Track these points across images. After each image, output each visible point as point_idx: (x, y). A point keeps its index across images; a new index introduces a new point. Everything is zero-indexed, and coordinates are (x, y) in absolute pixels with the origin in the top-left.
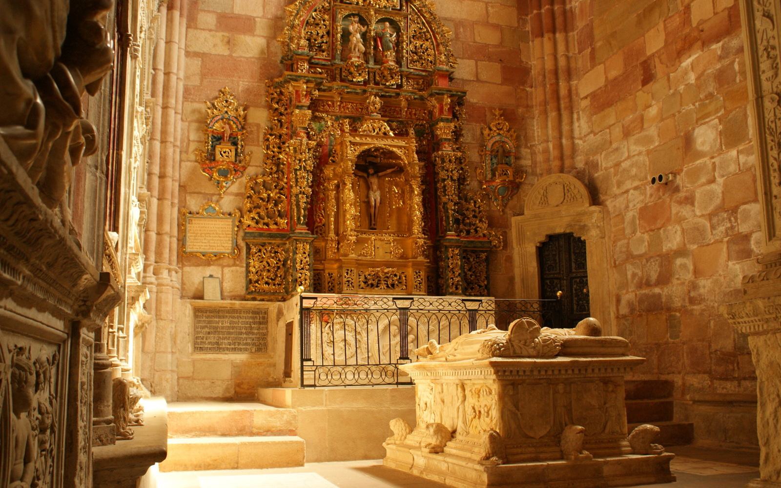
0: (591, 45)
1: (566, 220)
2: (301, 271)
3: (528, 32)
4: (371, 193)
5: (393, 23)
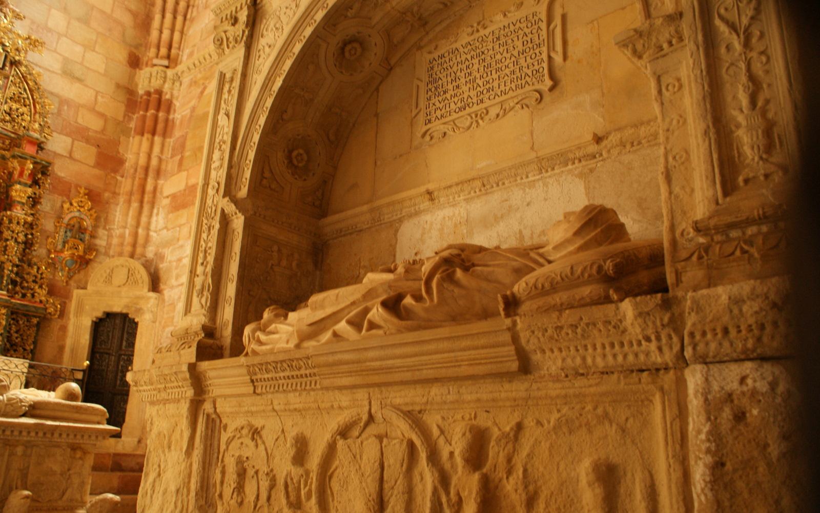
0: (182, 153)
1: (125, 301)
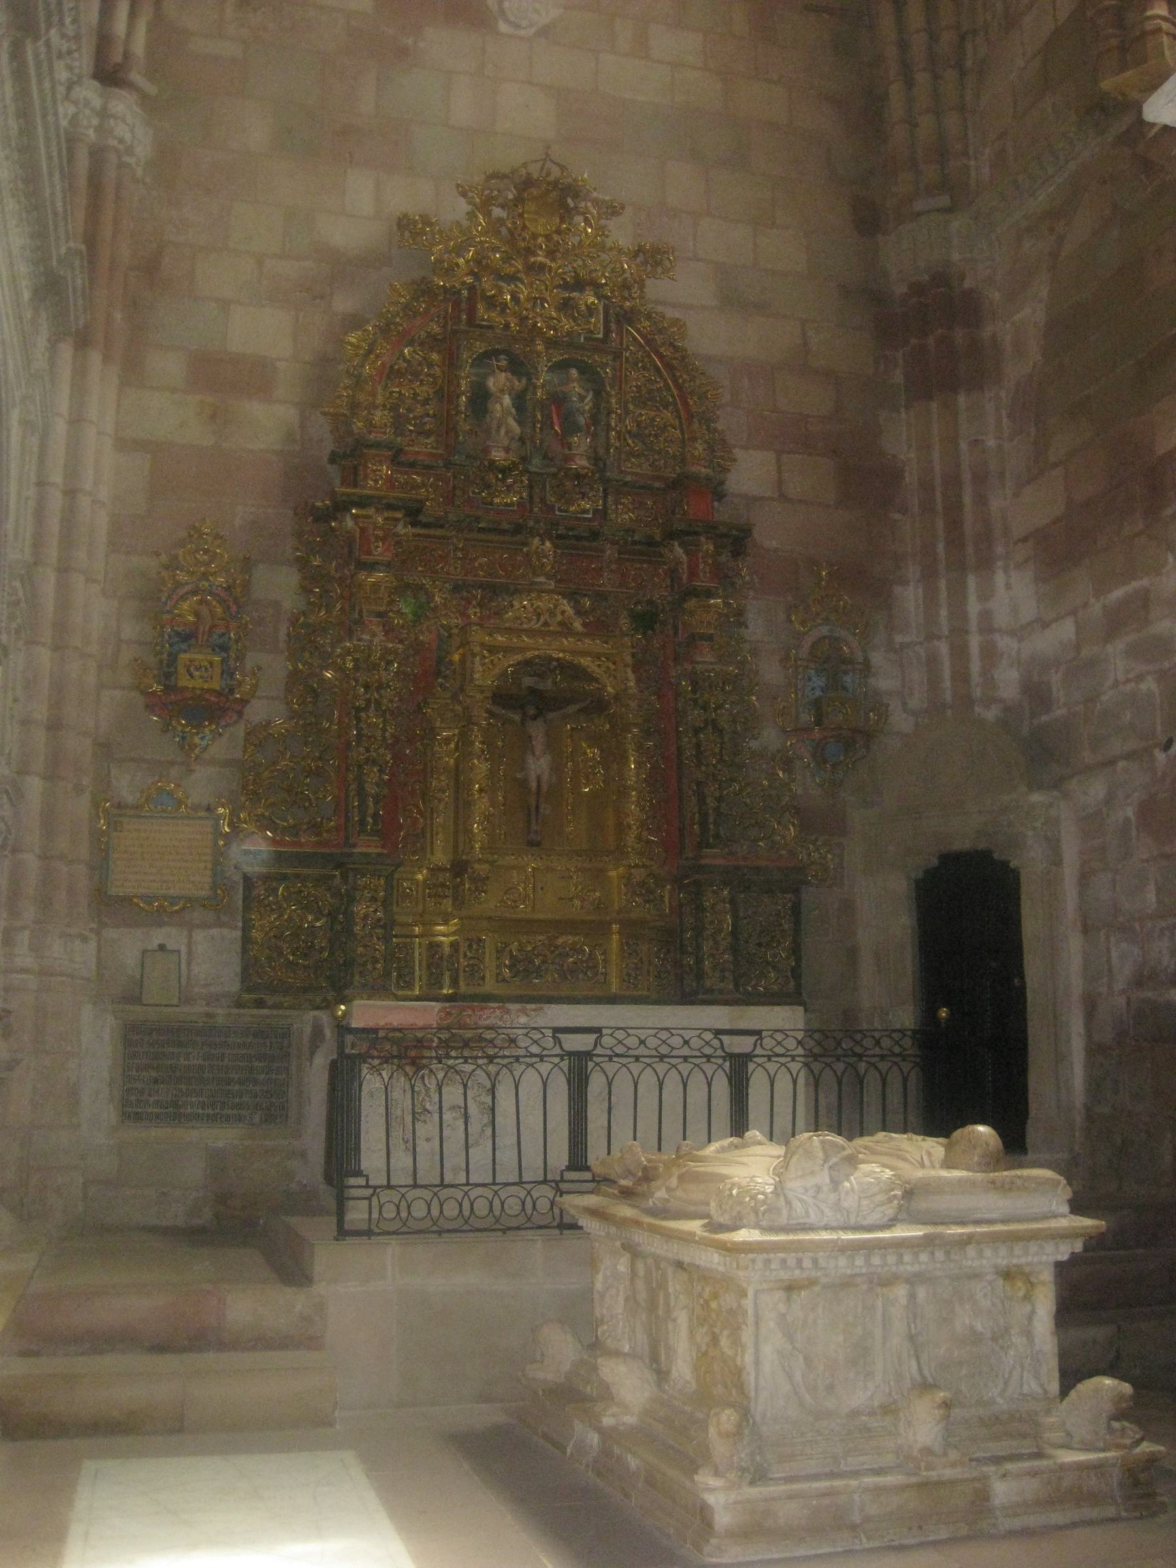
5: (584, 369)
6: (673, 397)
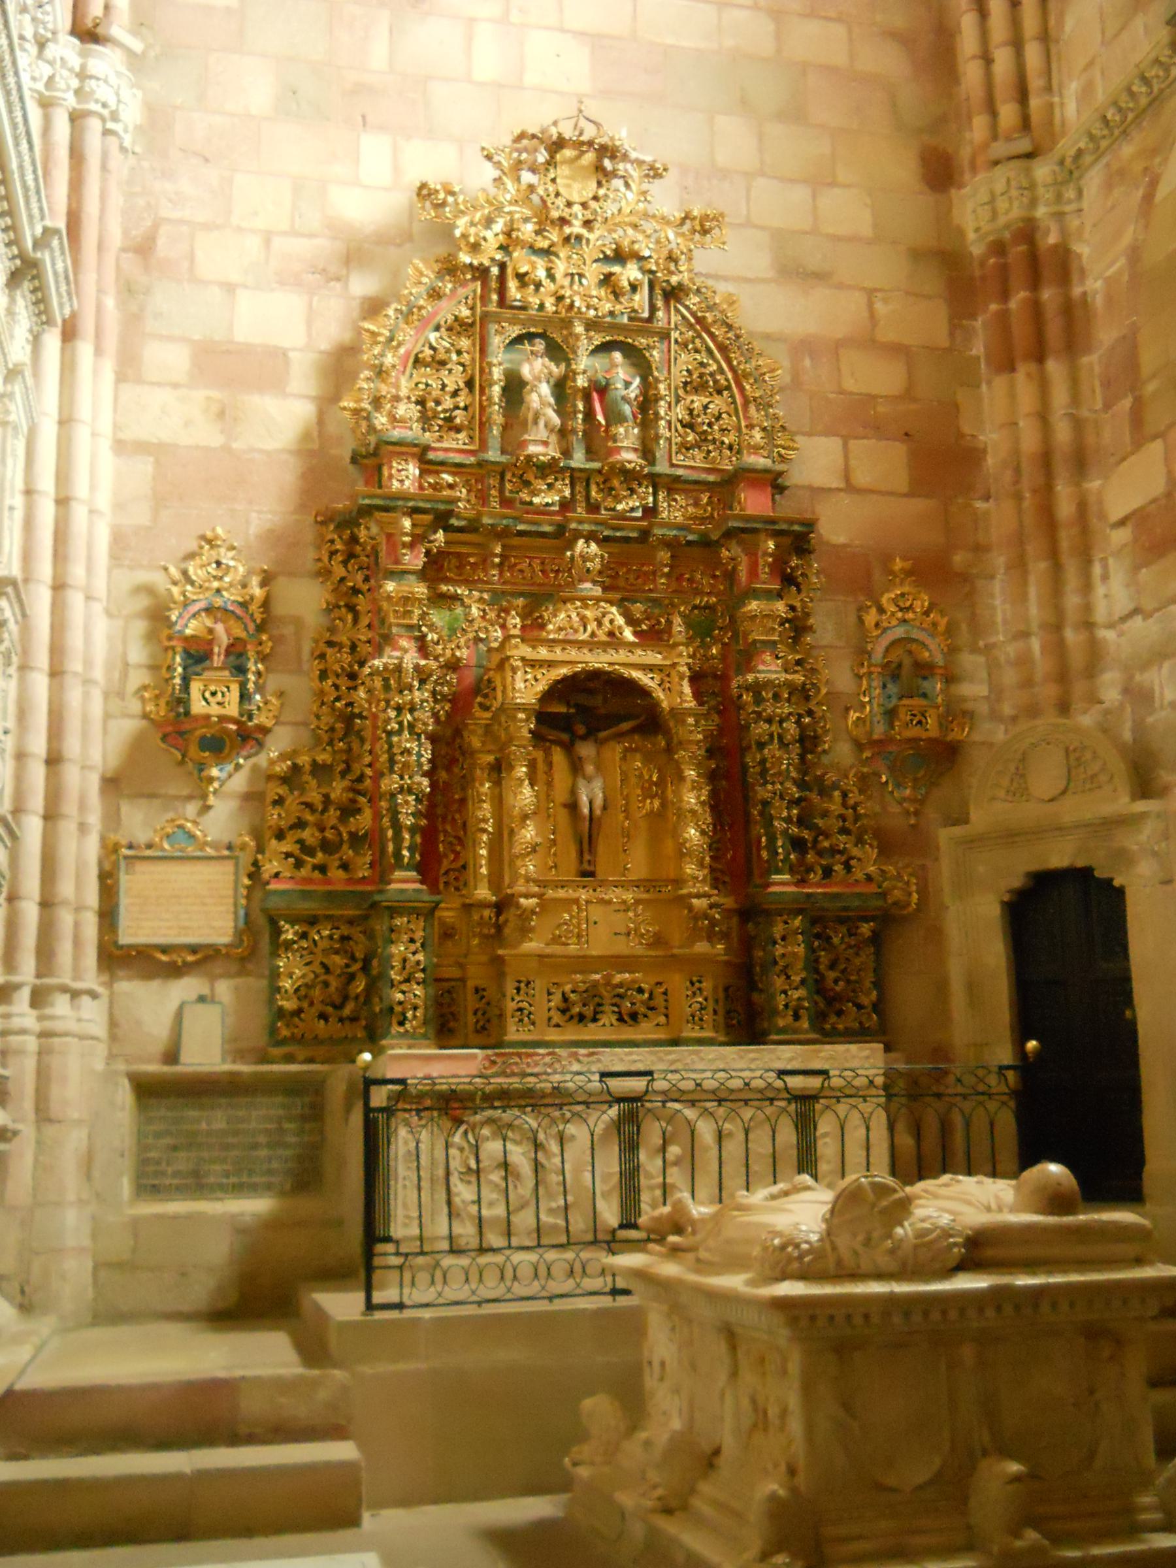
2: (404, 987)
3: (978, 358)
4: (582, 785)
6: (727, 380)
